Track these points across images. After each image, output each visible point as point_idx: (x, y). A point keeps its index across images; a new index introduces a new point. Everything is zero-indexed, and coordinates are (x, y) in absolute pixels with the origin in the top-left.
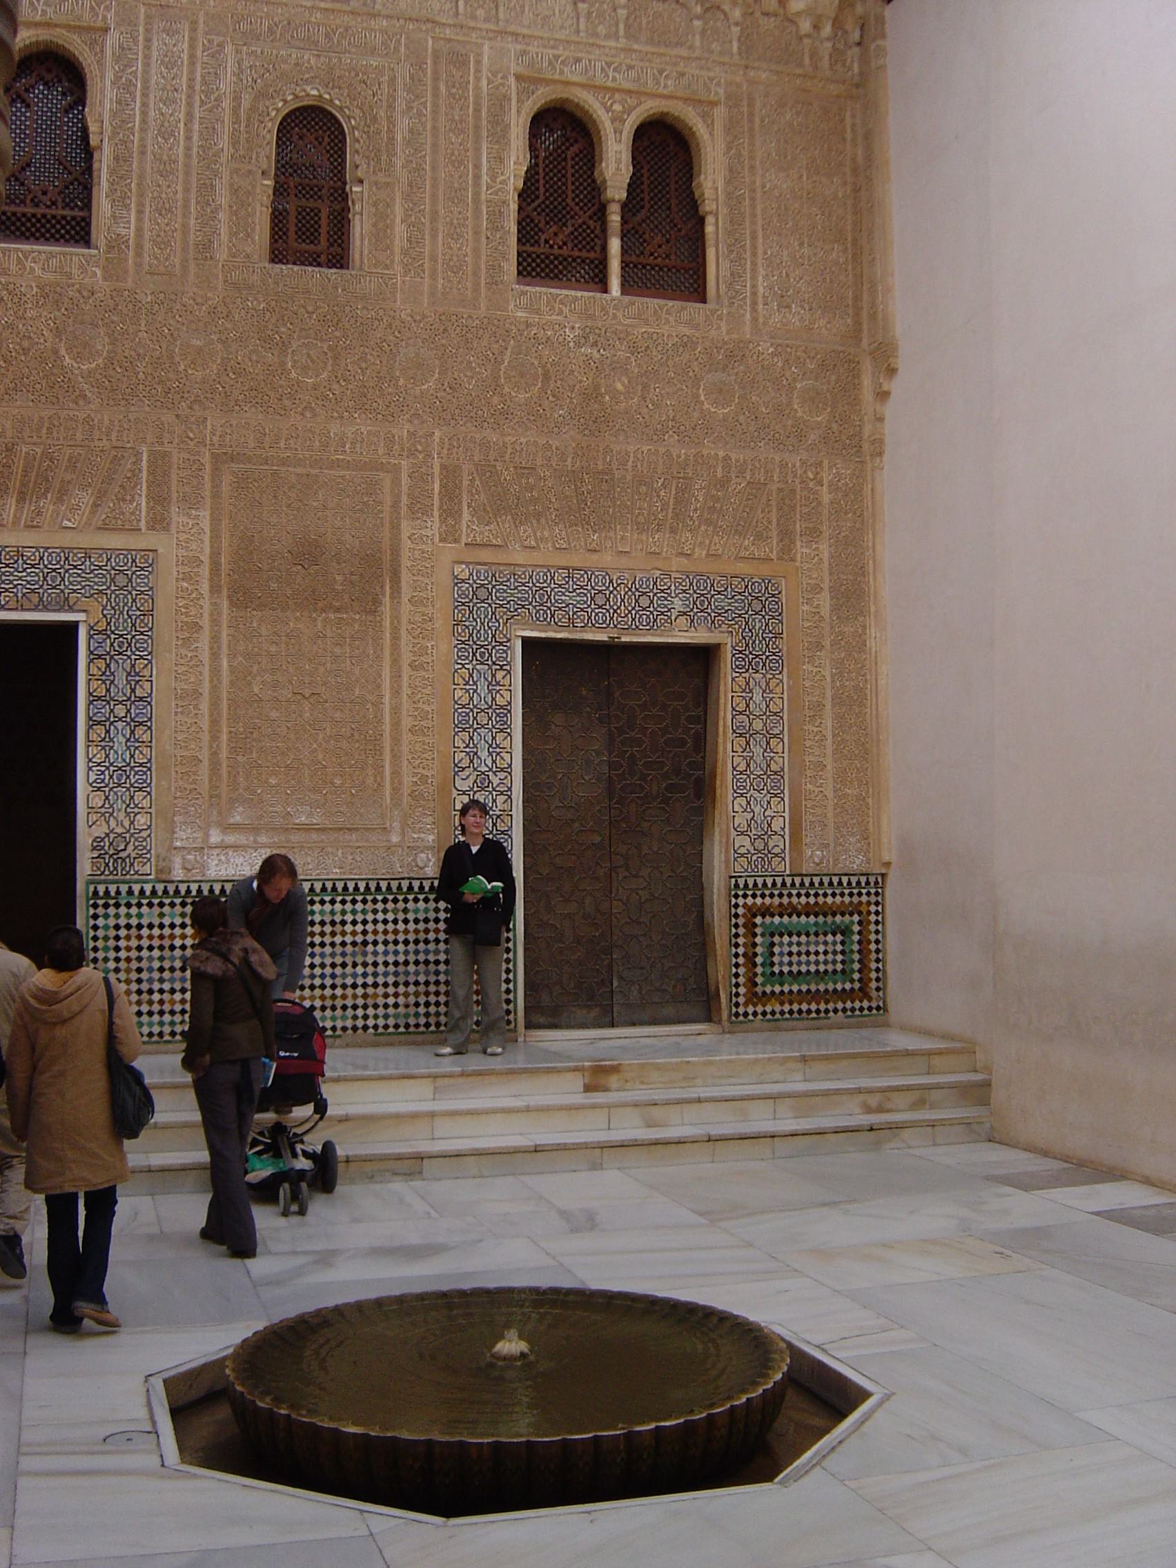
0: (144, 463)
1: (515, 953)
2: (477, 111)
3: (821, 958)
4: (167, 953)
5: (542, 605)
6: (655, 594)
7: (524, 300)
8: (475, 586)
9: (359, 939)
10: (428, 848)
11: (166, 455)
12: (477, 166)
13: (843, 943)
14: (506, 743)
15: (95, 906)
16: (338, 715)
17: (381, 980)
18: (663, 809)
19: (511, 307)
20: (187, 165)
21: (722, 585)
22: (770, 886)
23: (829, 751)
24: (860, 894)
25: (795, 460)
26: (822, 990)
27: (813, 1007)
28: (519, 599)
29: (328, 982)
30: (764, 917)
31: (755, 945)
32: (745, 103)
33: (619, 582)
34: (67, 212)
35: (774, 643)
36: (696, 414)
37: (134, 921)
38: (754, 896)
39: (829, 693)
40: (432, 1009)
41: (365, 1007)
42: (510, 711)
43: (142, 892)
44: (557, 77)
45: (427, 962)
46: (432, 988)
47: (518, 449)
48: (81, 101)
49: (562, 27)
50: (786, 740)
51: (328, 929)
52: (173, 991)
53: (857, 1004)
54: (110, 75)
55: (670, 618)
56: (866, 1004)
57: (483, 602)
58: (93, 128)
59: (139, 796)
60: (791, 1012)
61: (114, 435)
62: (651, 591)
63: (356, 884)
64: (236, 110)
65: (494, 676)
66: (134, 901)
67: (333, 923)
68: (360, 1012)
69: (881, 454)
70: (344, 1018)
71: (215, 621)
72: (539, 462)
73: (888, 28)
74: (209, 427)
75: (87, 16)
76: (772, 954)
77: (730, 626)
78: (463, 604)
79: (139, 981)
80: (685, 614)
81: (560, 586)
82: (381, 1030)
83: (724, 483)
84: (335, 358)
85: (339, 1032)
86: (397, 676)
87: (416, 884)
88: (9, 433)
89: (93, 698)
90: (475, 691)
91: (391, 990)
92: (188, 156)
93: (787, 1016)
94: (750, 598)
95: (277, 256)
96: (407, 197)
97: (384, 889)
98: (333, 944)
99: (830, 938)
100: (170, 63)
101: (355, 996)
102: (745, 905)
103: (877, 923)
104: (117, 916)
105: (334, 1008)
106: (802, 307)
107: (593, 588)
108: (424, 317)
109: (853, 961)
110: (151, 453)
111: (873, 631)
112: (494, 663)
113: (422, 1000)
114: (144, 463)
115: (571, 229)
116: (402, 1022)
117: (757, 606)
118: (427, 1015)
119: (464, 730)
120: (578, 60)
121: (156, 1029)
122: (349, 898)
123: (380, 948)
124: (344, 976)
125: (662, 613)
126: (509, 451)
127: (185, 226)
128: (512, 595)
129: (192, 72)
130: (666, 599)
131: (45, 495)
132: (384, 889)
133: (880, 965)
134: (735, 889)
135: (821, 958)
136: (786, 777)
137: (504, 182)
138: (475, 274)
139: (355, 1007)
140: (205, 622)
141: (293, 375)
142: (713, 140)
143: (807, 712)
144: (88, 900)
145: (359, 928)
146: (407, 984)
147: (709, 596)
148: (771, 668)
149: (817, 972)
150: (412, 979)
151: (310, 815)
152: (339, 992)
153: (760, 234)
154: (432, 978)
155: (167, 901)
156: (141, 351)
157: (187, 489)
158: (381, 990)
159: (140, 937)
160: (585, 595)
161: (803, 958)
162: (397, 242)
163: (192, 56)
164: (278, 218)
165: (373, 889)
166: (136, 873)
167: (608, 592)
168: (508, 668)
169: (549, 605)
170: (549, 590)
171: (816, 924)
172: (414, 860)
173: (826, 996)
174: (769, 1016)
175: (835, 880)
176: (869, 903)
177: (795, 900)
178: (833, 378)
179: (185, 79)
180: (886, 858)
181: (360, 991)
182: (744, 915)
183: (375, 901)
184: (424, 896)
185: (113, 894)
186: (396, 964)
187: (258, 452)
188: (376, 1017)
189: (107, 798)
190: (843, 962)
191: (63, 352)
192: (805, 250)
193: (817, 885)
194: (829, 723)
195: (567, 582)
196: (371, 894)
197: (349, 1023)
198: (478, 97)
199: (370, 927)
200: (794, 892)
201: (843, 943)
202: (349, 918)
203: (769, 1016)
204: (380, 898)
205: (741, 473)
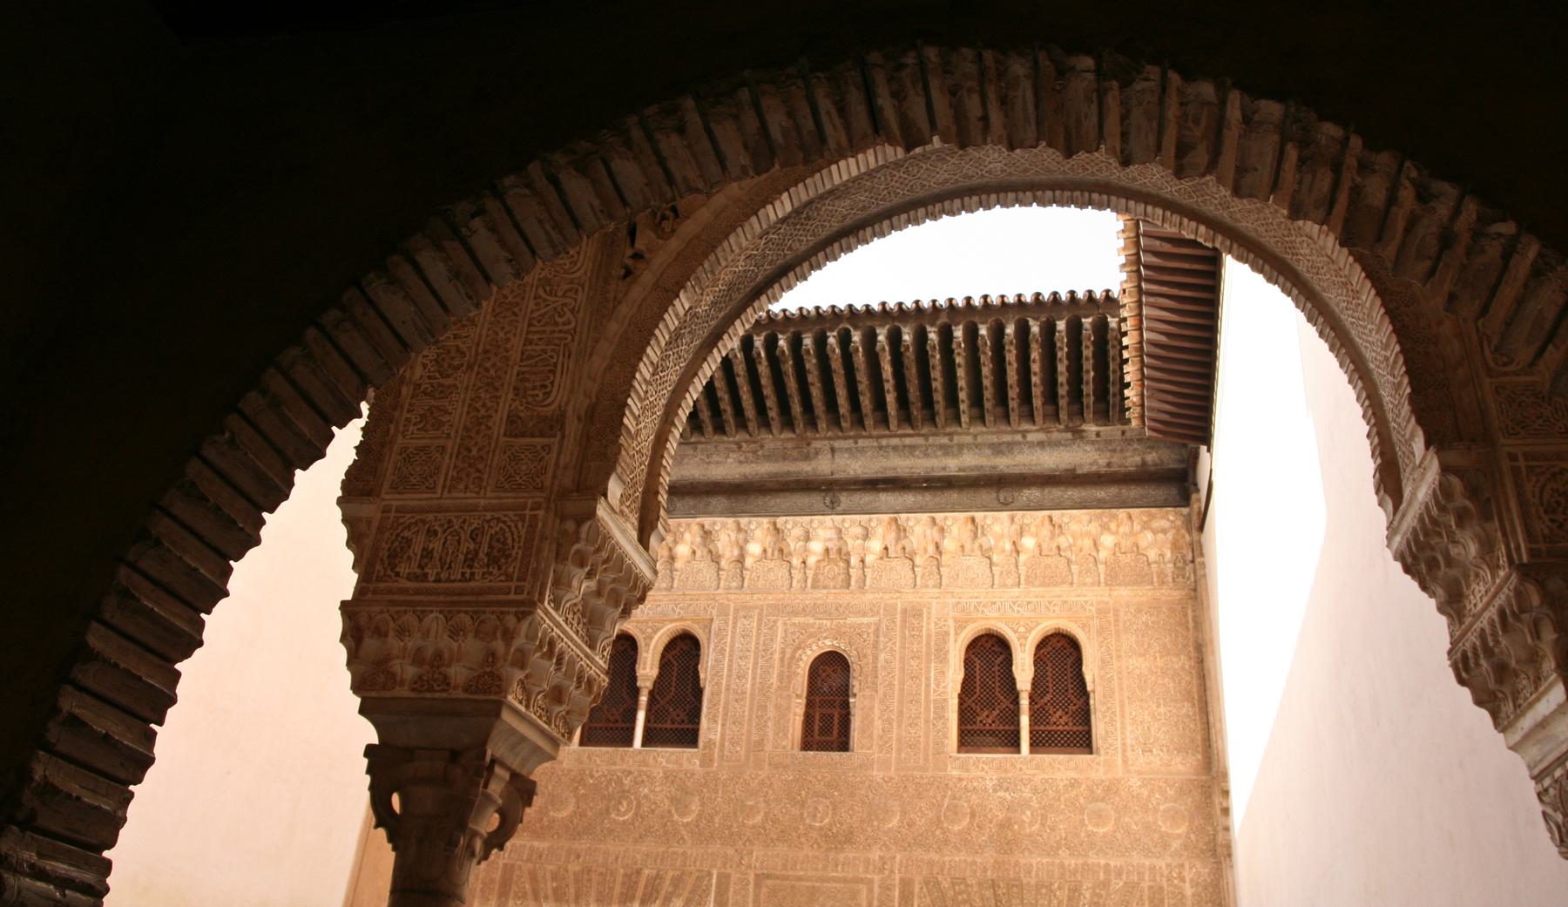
0: (714, 881)
2: (928, 643)
11: (728, 876)
12: (928, 679)
19: (949, 768)
20: (752, 695)
25: (1161, 864)
32: (1111, 614)
36: (1083, 835)
44: (980, 615)
47: (953, 864)
49: (984, 584)
54: (712, 646)
58: (702, 676)
61: (698, 864)
64: (782, 659)
69: (1230, 855)
72: (968, 873)
73: (1204, 551)
74: (754, 858)
83: (1105, 884)
84: (834, 809)
88: (639, 862)
92: (753, 689)
95: (806, 746)
96: (882, 702)
106: (1162, 750)
108: (891, 779)
114: (714, 881)
115: (998, 712)
120: (994, 603)
126: (947, 866)
137: (945, 687)
141: (808, 821)
156: (717, 809)
178: (1190, 799)
179: (753, 643)
187: (783, 872)
191: (673, 811)
192: (1162, 710)
205: (1119, 874)
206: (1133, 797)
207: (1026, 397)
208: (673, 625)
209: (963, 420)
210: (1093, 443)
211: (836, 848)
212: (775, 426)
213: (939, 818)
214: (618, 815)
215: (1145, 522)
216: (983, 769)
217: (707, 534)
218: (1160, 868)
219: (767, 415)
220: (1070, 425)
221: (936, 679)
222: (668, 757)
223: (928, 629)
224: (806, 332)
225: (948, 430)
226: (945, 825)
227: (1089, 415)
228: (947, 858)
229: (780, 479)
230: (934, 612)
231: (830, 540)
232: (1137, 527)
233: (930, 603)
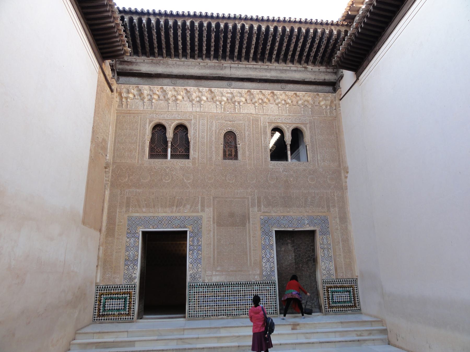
2: (261, 129)
3: (344, 298)
4: (204, 298)
7: (272, 164)
9: (244, 294)
10: (257, 275)
11: (204, 198)
12: (261, 140)
14: (273, 252)
15: (190, 288)
16: (238, 247)
17: (248, 303)
18: (307, 265)
20: (207, 143)
24: (352, 283)
27: (344, 309)
29: (238, 304)
30: (330, 288)
31: (329, 295)
34: (186, 153)
37: (198, 291)
38: (328, 284)
39: (340, 239)
41: (245, 309)
43: (199, 285)
44: (276, 122)
48: (187, 133)
50: (332, 249)
51: (237, 292)
52: (205, 306)
53: (354, 309)
54: (192, 128)
56: (356, 309)
58: (189, 138)
59: (199, 265)
60: (339, 310)
61: (194, 194)
64: (216, 133)
65: (269, 238)
66: (198, 287)
67: (238, 291)
68: (244, 311)
70: (241, 312)
71: (214, 229)
75: (188, 118)
79: (199, 304)
80: (308, 224)
83: (314, 197)
85: (240, 315)
86: (250, 239)
89: (190, 245)
92: (207, 142)
98: (238, 296)
100: (203, 125)
103: (356, 290)
104: (194, 290)
109: (352, 299)
110: (201, 197)
117: (323, 222)
120: (280, 118)
121: (202, 315)
122: (241, 285)
123: (248, 296)
124: (241, 302)
127: (207, 155)
129: (207, 126)
131: (181, 206)
132: (249, 283)
133: (358, 299)
134: (324, 282)
135: (344, 298)
138: (262, 160)
139: (243, 309)
140: (212, 230)
141: (228, 181)
142: (307, 131)
144: (189, 287)
145: (244, 292)
149: (344, 301)
152: (240, 306)
153: (318, 147)
155: (204, 287)
157: (208, 204)
158: (248, 306)
159: (199, 295)
161: (340, 298)
162: (247, 155)
163: (207, 124)
164: (224, 152)
165: (246, 284)
166: (198, 281)
171: (342, 290)
172: (255, 277)
174: (334, 311)
176: (354, 285)
177: (337, 285)
180: (357, 275)
181: (244, 306)
182: (326, 288)
183: (247, 286)
185: (194, 285)
189: (193, 265)
190: (350, 299)
191: (184, 179)
193: (342, 281)
194: (341, 245)
197: (242, 313)
198: (261, 127)
199: (246, 292)
200: (337, 283)
201: (349, 294)
202: (242, 290)
203: (334, 311)
204: (248, 285)
206: (321, 174)
207: (293, 55)
208: (178, 121)
209: (272, 61)
210: (310, 72)
211: (237, 189)
212: (212, 57)
213: (267, 179)
214: (165, 180)
215: (323, 97)
216: (279, 166)
217: (188, 92)
218: (329, 193)
219: (210, 53)
220: (304, 66)
221: (264, 140)
222: (180, 163)
223: (260, 125)
224: (230, 23)
225: (267, 64)
226: (269, 182)
227: (310, 63)
228: (270, 191)
229: (214, 76)
230: (262, 120)
231: (229, 97)
232: (321, 99)
233: (261, 117)
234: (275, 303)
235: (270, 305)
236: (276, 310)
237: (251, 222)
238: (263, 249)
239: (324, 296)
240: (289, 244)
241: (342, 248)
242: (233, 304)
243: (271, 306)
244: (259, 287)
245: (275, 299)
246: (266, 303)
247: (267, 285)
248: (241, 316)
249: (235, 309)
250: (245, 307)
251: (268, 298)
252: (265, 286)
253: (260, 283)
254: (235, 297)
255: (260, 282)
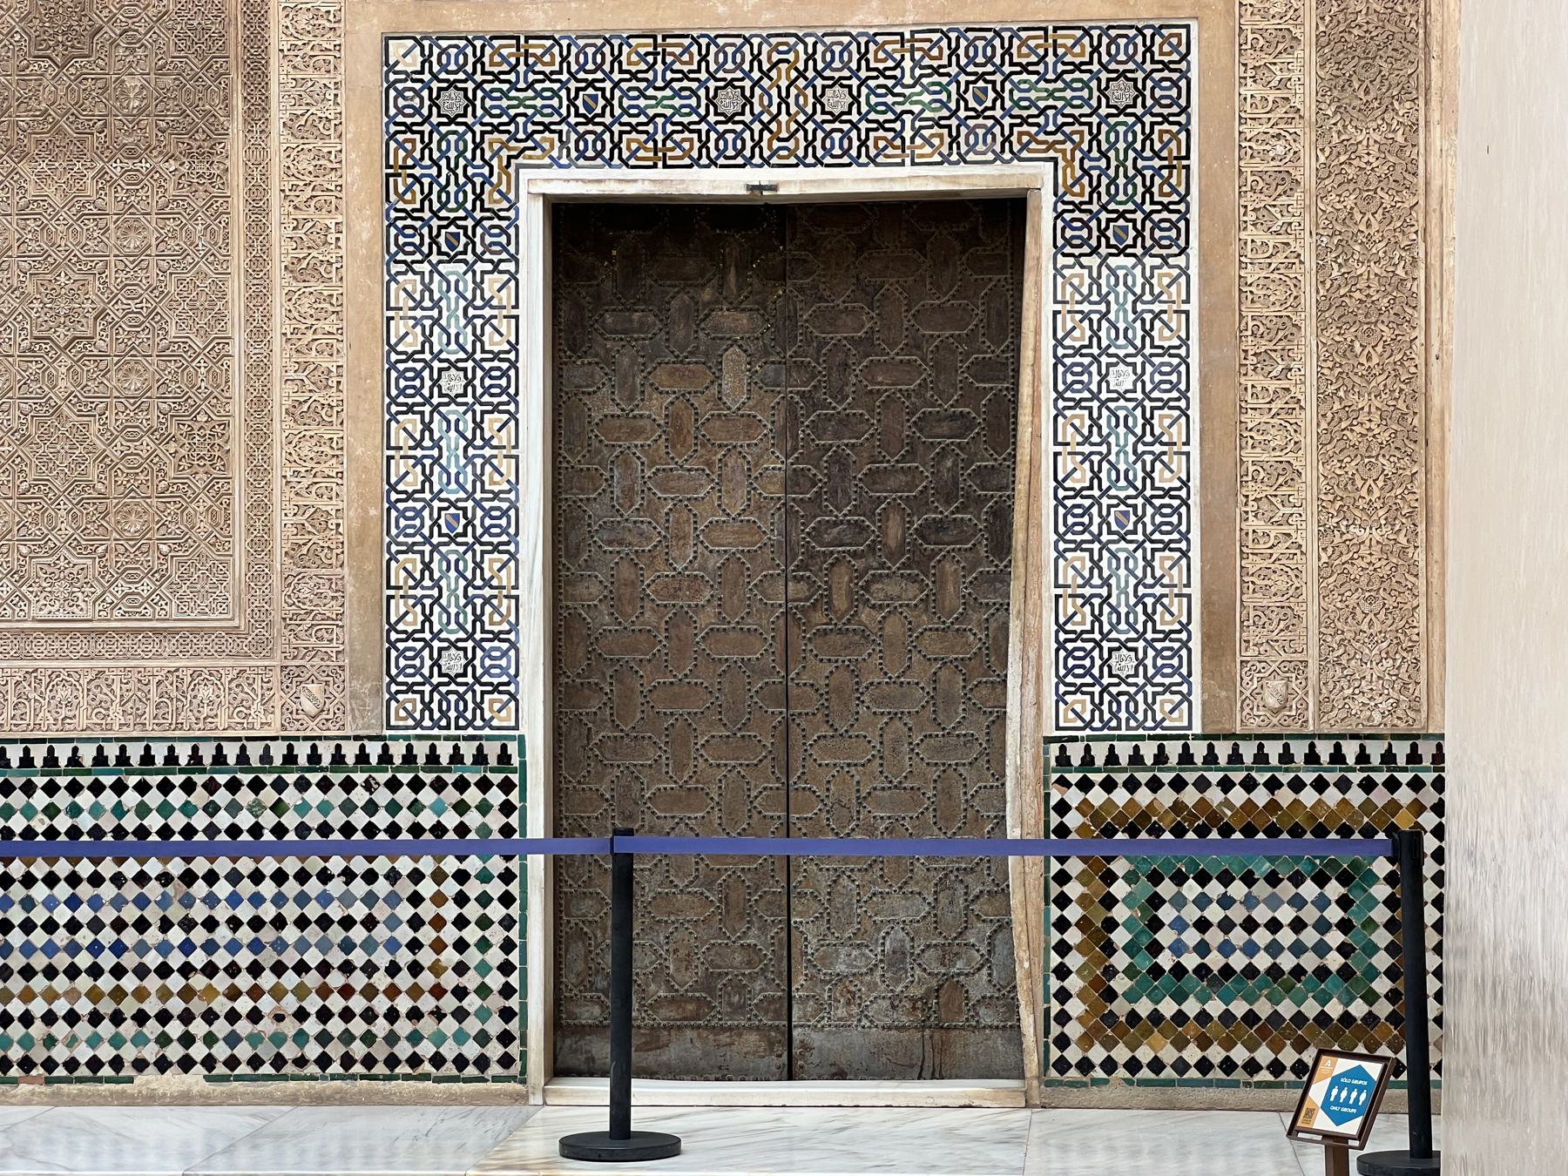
1: (524, 907)
3: (1286, 937)
5: (590, 121)
6: (863, 82)
8: (435, 85)
13: (1344, 903)
16: (135, 383)
17: (222, 959)
18: (913, 579)
21: (1033, 51)
22: (1149, 761)
23: (1309, 440)
24: (1392, 785)
26: (1288, 1016)
28: (538, 111)
29: (107, 960)
31: (1109, 901)
33: (775, 57)
35: (1166, 181)
38: (1109, 785)
39: (1309, 299)
40: (335, 1026)
41: (187, 1017)
42: (514, 365)
45: (324, 922)
46: (336, 979)
50: (1194, 413)
55: (899, 134)
57: (452, 121)
60: (1204, 1066)
62: (855, 74)
63: (171, 749)
65: (478, 285)
68: (175, 1029)
70: (139, 1040)
76: (1156, 925)
77: (1051, 146)
78: (409, 128)
81: (634, 76)
82: (221, 1069)
85: (127, 1071)
86: (258, 295)
87: (302, 751)
90: (436, 322)
91: (244, 981)
93: (1193, 1074)
94: (1104, 76)
97: (232, 760)
99: (1309, 890)
101: (165, 994)
102: (1084, 807)
105: (117, 1019)
107: (712, 76)
109: (1372, 949)
111: (1436, 132)
112: (479, 258)
113: (313, 1004)
116: (266, 1053)
117: (1121, 93)
118: (324, 1038)
119: (410, 409)
122: (154, 780)
123: (223, 889)
124: (142, 949)
125: (881, 125)
128: (521, 103)
130: (890, 91)
132: (232, 760)
135: (1286, 937)
136: (1194, 501)
139: (164, 1017)
143: (1249, 343)
146: (279, 969)
147: (998, 78)
148: (1156, 243)
149: (1275, 971)
150: (291, 958)
151: (71, 600)
152: (129, 983)
154: (336, 958)
160: (694, 93)
161: (1238, 936)
165: (207, 761)
167: (747, 84)
168: (511, 266)
169: (608, 120)
170: (608, 85)
173: (1297, 1030)
174: (1145, 1073)
175: (1324, 749)
176: (1417, 807)
177: (1215, 796)
181: (175, 982)
183: (211, 787)
184: (320, 776)
186: (256, 924)
188: (210, 1040)
190: (1344, 950)
193: (1274, 761)
195: (651, 67)
196: (203, 771)
197: (151, 1052)
200: (1214, 777)
201: (1344, 903)
203: (1145, 1073)
204: (222, 779)
234: (506, 968)
235: (450, 980)
236: (506, 1038)
237: (278, 113)
238: (398, 402)
239: (1055, 913)
240: (733, 356)
241: (1323, 398)
242: (62, 961)
243: (460, 993)
244: (337, 795)
245: (507, 923)
246: (404, 957)
247: (428, 778)
248: (140, 1079)
249: (84, 1007)
250: (187, 993)
251: (427, 911)
252: (405, 796)
253: (350, 760)
254: (85, 890)
255: (350, 751)
